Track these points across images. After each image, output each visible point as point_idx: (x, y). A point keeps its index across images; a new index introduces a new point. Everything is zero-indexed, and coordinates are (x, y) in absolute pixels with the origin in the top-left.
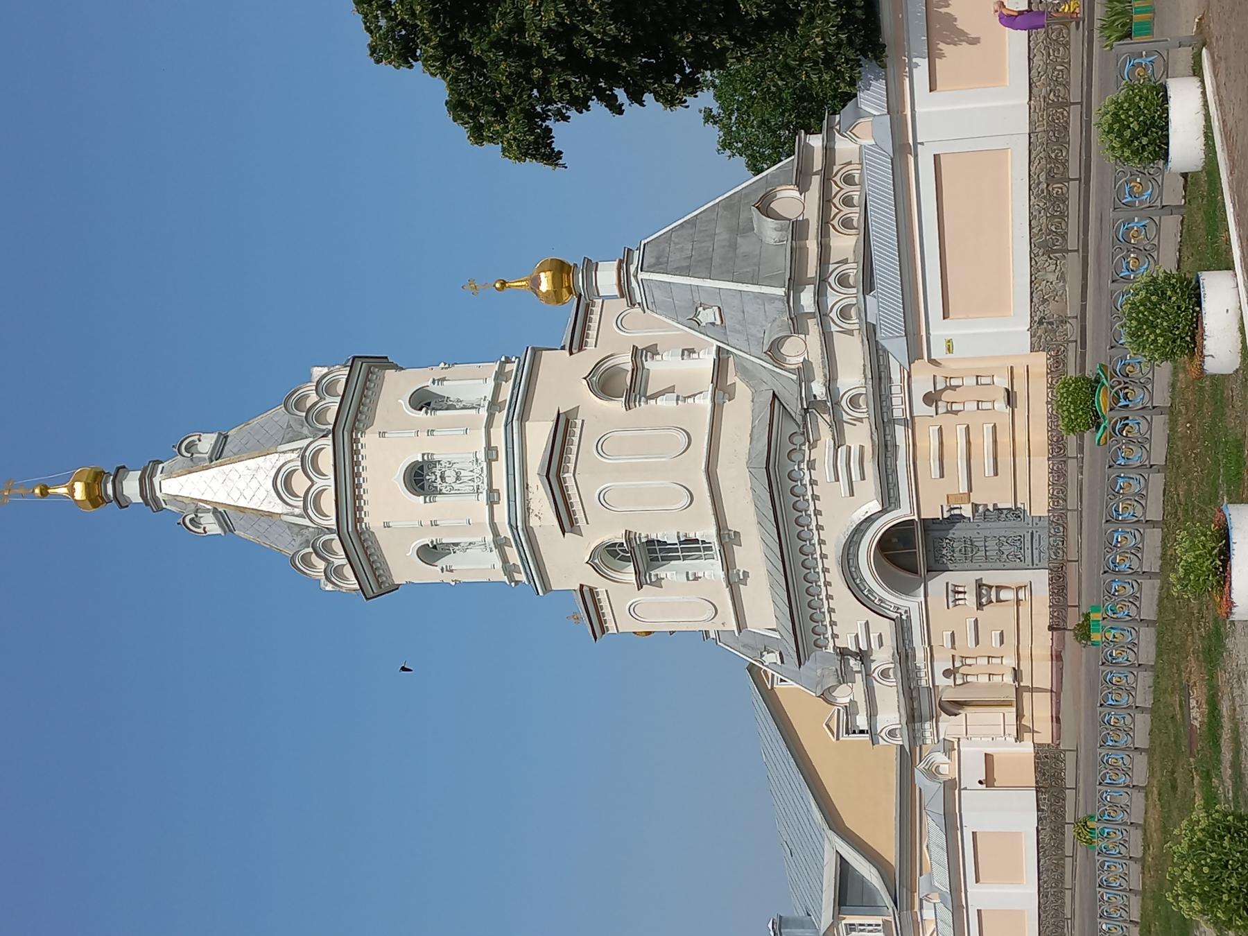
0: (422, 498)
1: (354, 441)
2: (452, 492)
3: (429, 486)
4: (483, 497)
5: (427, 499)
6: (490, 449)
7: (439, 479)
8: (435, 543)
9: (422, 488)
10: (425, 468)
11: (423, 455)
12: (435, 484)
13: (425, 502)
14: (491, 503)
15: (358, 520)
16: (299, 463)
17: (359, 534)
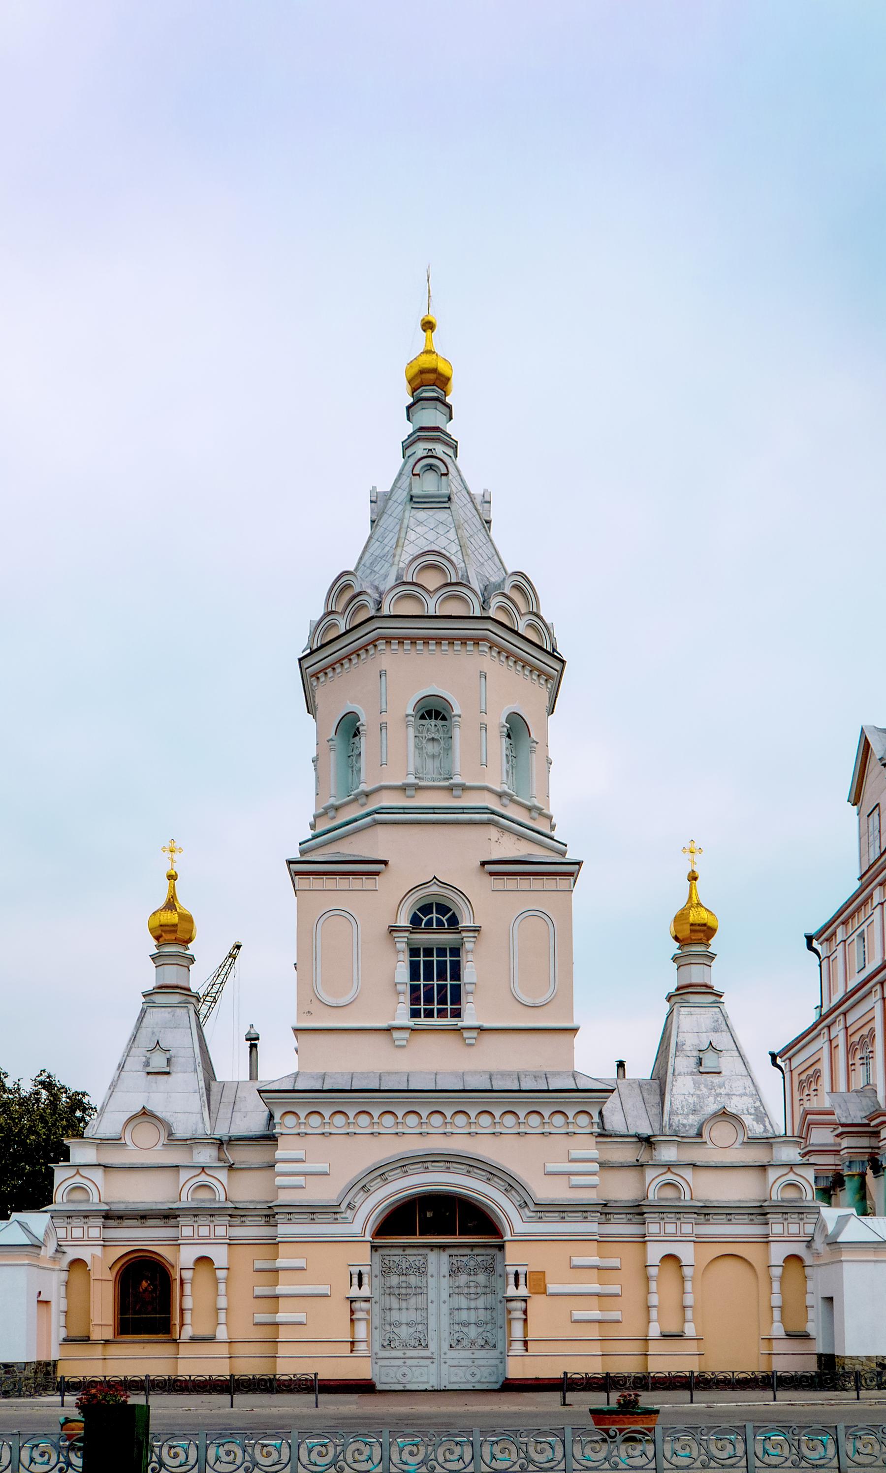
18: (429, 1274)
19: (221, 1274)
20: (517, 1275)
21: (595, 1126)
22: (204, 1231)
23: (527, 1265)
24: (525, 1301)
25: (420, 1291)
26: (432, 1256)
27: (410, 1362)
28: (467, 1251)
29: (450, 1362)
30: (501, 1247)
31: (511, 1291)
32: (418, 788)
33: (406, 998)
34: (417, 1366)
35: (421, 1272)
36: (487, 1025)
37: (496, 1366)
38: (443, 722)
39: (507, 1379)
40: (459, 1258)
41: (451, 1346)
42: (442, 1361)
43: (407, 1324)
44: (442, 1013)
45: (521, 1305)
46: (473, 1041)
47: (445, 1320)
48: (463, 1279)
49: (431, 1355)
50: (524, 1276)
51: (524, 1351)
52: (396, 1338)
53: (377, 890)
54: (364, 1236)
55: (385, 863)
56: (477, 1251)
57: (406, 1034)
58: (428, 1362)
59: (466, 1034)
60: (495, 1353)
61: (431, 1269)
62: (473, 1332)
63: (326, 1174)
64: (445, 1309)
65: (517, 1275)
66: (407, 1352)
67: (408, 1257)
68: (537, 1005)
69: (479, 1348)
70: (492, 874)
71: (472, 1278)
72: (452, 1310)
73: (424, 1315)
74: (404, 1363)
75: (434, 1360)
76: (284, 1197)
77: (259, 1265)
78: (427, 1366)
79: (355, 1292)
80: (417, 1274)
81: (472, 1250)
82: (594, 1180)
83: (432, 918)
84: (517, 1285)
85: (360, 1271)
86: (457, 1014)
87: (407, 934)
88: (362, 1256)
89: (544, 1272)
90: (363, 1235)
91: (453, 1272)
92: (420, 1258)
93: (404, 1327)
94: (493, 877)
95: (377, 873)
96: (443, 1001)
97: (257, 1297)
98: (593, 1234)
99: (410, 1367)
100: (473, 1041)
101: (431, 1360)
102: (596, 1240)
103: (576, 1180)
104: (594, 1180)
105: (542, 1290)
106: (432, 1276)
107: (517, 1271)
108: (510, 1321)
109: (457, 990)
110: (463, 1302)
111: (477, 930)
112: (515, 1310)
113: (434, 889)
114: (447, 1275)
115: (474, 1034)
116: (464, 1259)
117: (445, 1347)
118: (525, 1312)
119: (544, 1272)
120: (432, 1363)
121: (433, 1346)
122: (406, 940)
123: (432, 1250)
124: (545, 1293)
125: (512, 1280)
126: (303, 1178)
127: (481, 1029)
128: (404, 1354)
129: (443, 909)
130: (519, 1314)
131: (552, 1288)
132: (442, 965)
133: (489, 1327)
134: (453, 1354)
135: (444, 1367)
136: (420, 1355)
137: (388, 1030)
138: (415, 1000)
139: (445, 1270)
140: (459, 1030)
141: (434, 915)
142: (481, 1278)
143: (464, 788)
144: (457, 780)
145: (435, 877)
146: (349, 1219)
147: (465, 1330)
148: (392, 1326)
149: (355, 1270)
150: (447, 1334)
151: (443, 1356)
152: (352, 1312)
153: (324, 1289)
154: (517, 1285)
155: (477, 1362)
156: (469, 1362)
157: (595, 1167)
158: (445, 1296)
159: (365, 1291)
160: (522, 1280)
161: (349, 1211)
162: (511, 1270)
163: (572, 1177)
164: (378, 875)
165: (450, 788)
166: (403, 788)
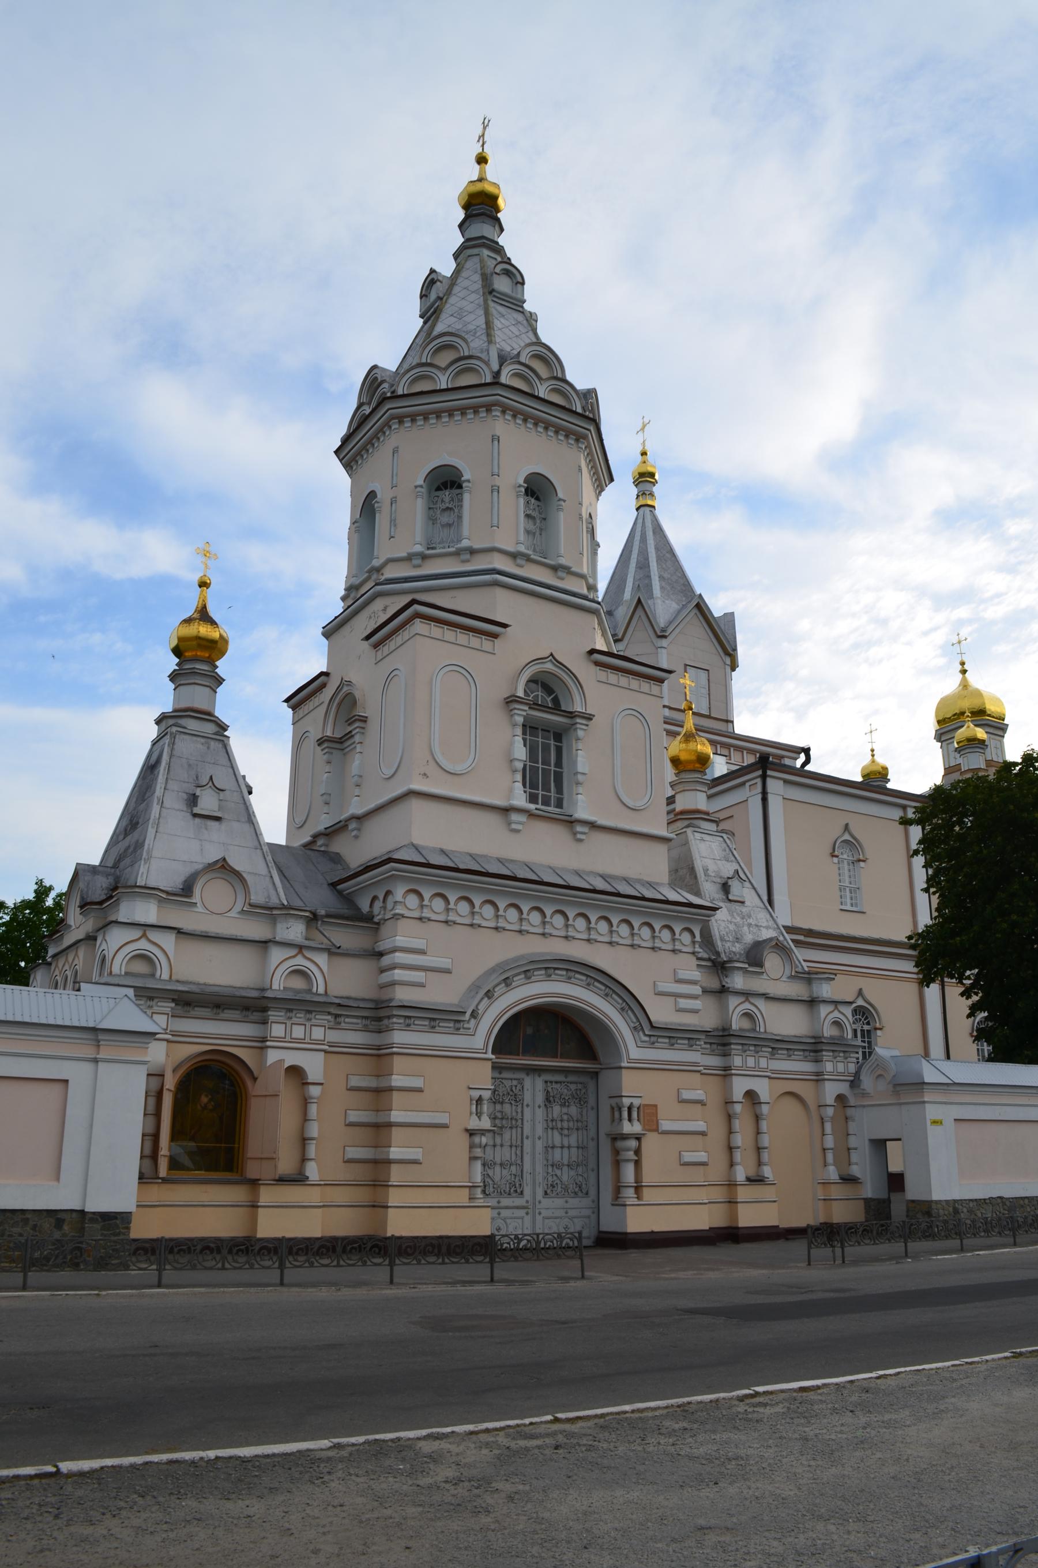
0: (420, 482)
1: (489, 408)
2: (432, 520)
3: (438, 497)
4: (418, 548)
5: (419, 489)
6: (472, 552)
7: (444, 506)
8: (376, 505)
9: (438, 489)
10: (458, 491)
11: (468, 481)
12: (440, 500)
13: (416, 487)
14: (409, 558)
15: (401, 420)
16: (466, 354)
17: (387, 424)
18: (525, 1104)
19: (314, 1091)
20: (630, 1109)
21: (697, 946)
22: (298, 1032)
23: (641, 1097)
24: (638, 1138)
25: (515, 1123)
26: (528, 1082)
27: (505, 1213)
28: (560, 1078)
29: (544, 1213)
30: (595, 1075)
31: (627, 1128)
32: (528, 559)
33: (519, 777)
34: (511, 1218)
35: (516, 1099)
36: (602, 821)
37: (589, 1217)
38: (537, 503)
39: (600, 1232)
40: (554, 1086)
41: (546, 1193)
42: (537, 1211)
43: (501, 1165)
44: (546, 802)
45: (633, 1143)
46: (582, 837)
47: (540, 1158)
48: (557, 1110)
49: (525, 1204)
50: (636, 1109)
51: (636, 1200)
52: (491, 1182)
53: (494, 654)
54: (486, 1053)
55: (505, 626)
56: (571, 1078)
57: (522, 818)
58: (521, 1213)
59: (579, 828)
60: (586, 1202)
61: (527, 1097)
62: (566, 1175)
63: (448, 971)
64: (539, 1145)
65: (630, 1109)
66: (502, 1200)
67: (503, 1081)
68: (637, 808)
69: (572, 1195)
70: (597, 663)
71: (565, 1110)
72: (549, 1148)
73: (519, 1153)
74: (499, 1214)
75: (529, 1211)
76: (402, 995)
77: (355, 1082)
78: (522, 1218)
79: (474, 1123)
80: (513, 1102)
81: (566, 1077)
82: (696, 1004)
83: (538, 695)
84: (630, 1120)
85: (480, 1096)
86: (559, 804)
87: (526, 708)
88: (482, 1076)
89: (656, 1106)
90: (484, 1051)
91: (548, 1100)
92: (515, 1083)
93: (498, 1168)
94: (598, 668)
95: (495, 636)
96: (546, 788)
97: (351, 1125)
98: (695, 1064)
99: (504, 1219)
100: (582, 837)
101: (525, 1211)
102: (698, 1071)
103: (683, 1003)
104: (696, 1004)
105: (654, 1127)
106: (528, 1106)
107: (632, 1103)
108: (617, 1164)
109: (559, 778)
110: (557, 1139)
111: (589, 718)
112: (628, 1150)
113: (549, 666)
114: (542, 1105)
115: (585, 829)
116: (558, 1086)
117: (540, 1192)
118: (638, 1152)
119: (656, 1106)
120: (527, 1214)
121: (527, 1191)
122: (524, 713)
123: (528, 1074)
124: (656, 1130)
125: (625, 1114)
126: (423, 974)
127: (593, 826)
128: (499, 1202)
129: (548, 690)
130: (631, 1155)
131: (665, 1125)
132: (546, 748)
133: (580, 1170)
134: (546, 1202)
135: (539, 1218)
136: (514, 1204)
137: (506, 811)
138: (524, 785)
139: (540, 1098)
140: (572, 822)
141: (540, 693)
142: (573, 1110)
143: (567, 570)
144: (563, 561)
145: (552, 655)
146: (471, 1030)
147: (558, 1172)
148: (487, 1167)
149: (476, 1094)
150: (540, 1178)
151: (538, 1206)
152: (472, 1146)
153: (442, 1118)
154: (630, 1120)
155: (572, 1213)
156: (561, 1213)
157: (697, 990)
158: (539, 1130)
159: (486, 1123)
160: (635, 1115)
161: (473, 1020)
162: (626, 1102)
163: (678, 999)
164: (496, 638)
165: (555, 569)
166: (514, 556)
